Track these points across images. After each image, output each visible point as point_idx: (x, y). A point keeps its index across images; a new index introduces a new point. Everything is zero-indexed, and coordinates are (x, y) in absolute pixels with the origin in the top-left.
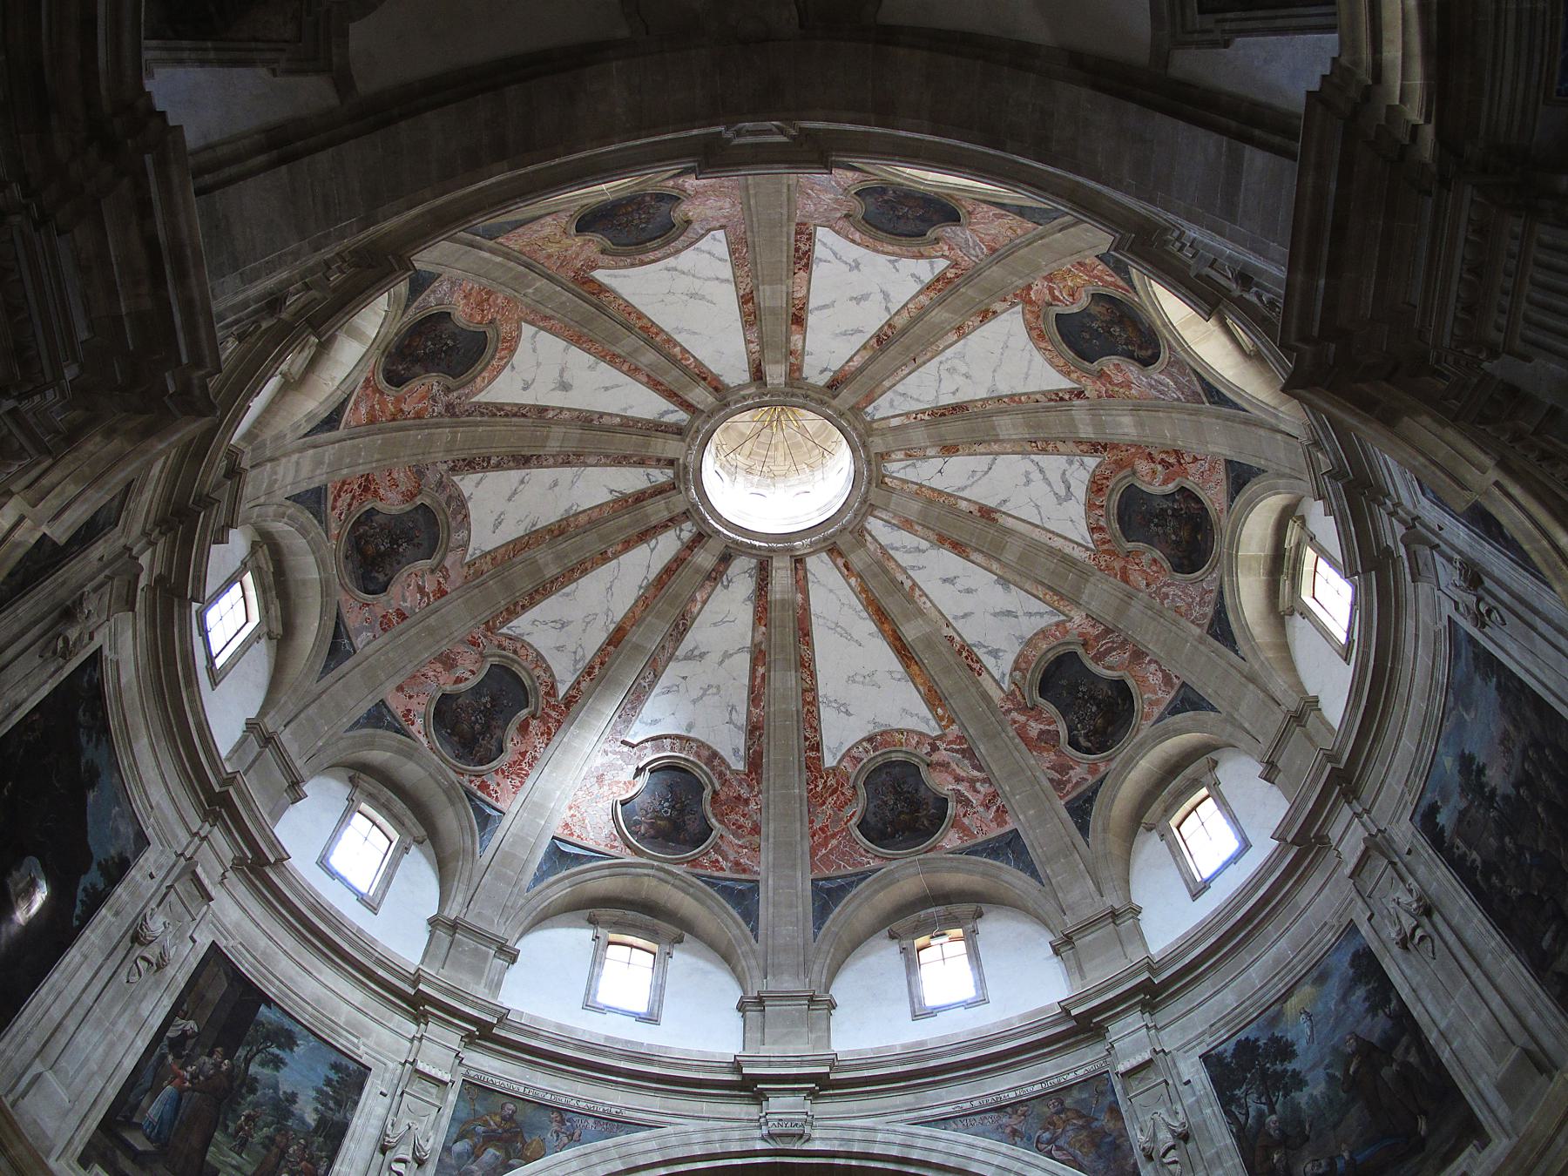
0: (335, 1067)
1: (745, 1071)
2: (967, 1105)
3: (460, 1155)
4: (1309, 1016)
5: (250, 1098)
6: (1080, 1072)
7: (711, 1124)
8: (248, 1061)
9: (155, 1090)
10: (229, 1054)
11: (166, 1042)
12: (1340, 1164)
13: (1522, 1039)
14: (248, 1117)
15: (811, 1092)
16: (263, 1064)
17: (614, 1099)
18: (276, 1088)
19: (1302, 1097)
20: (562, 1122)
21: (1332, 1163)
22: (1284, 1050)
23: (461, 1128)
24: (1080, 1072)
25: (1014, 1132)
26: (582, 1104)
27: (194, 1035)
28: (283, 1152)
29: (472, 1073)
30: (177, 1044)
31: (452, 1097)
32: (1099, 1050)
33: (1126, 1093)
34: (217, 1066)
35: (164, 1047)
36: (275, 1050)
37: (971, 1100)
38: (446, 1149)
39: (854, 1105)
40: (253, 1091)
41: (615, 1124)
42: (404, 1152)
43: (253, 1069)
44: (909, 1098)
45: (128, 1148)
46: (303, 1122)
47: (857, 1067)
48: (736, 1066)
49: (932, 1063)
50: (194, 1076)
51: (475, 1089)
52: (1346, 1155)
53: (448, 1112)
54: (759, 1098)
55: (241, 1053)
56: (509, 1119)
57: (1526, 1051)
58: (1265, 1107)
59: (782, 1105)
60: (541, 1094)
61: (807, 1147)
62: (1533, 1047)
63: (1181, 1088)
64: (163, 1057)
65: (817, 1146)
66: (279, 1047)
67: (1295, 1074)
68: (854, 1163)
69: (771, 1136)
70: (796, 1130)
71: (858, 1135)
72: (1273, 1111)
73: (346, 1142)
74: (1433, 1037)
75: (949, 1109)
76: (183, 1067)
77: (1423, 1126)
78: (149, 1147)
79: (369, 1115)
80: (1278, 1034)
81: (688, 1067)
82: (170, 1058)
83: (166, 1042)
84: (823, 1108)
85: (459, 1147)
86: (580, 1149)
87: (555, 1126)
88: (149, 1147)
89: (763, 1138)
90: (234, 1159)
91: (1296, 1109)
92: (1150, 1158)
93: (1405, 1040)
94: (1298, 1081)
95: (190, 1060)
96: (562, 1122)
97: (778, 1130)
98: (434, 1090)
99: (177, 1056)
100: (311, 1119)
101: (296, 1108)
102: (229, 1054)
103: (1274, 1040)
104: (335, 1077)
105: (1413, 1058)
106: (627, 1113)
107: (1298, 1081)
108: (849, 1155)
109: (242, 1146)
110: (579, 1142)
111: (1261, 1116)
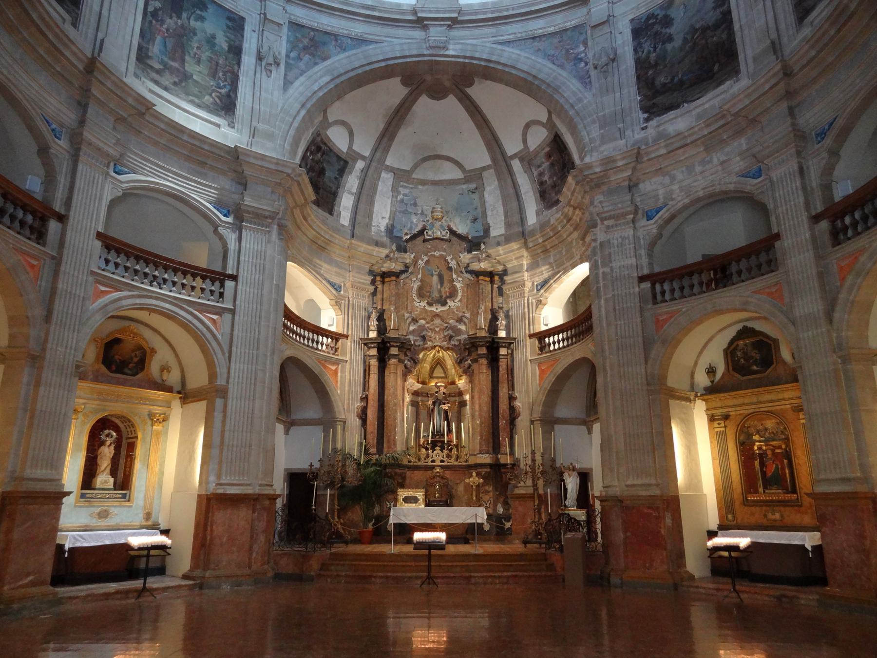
0: (229, 18)
1: (419, 15)
2: (519, 35)
3: (294, 59)
4: (685, 6)
5: (195, 38)
6: (573, 22)
7: (404, 41)
8: (189, 19)
9: (152, 40)
10: (179, 17)
11: (149, 14)
12: (676, 79)
13: (774, 36)
14: (198, 48)
15: (450, 26)
16: (196, 20)
17: (358, 29)
18: (206, 33)
19: (669, 47)
20: (336, 40)
21: (673, 79)
22: (667, 21)
23: (293, 45)
24: (573, 22)
25: (539, 50)
26: (345, 32)
27: (160, 9)
28: (217, 64)
29: (293, 17)
30: (155, 14)
31: (285, 29)
32: (583, 10)
33: (592, 33)
34: (176, 23)
35: (149, 18)
36: (199, 12)
37: (521, 33)
38: (287, 56)
39: (467, 33)
40: (195, 34)
41: (361, 41)
42: (271, 60)
43: (192, 22)
44: (493, 30)
45: (152, 67)
46: (221, 47)
47: (471, 14)
48: (415, 12)
49: (506, 13)
50: (167, 30)
51: (295, 26)
52: (680, 76)
53: (285, 38)
54: (425, 28)
55: (184, 15)
56: (312, 40)
57: (773, 43)
58: (652, 49)
59: (436, 33)
60: (325, 27)
61: (447, 53)
62: (777, 42)
63: (618, 35)
64: (151, 22)
65: (451, 53)
66: (201, 10)
67: (670, 35)
68: (467, 61)
69: (431, 47)
70: (442, 45)
71: (469, 48)
72: (655, 51)
73: (243, 56)
74: (736, 27)
75: (511, 37)
76: (161, 26)
77: (716, 68)
78: (161, 67)
79: (250, 43)
80: (668, 13)
81: (392, 12)
82: (154, 22)
83: (149, 14)
84: (455, 33)
85: (292, 55)
86: (347, 54)
87: (334, 43)
88: (161, 67)
89: (427, 48)
90: (198, 68)
91: (665, 51)
92: (596, 68)
93: (724, 26)
94: (670, 39)
95: (163, 22)
96: (336, 40)
97: (434, 44)
98: (277, 28)
99: (157, 21)
100: (225, 46)
101: (217, 41)
102: (179, 17)
103: (666, 17)
104: (230, 24)
105: (724, 36)
106: (365, 36)
107: (670, 39)
108: (465, 57)
109: (199, 62)
110: (345, 50)
111: (649, 52)
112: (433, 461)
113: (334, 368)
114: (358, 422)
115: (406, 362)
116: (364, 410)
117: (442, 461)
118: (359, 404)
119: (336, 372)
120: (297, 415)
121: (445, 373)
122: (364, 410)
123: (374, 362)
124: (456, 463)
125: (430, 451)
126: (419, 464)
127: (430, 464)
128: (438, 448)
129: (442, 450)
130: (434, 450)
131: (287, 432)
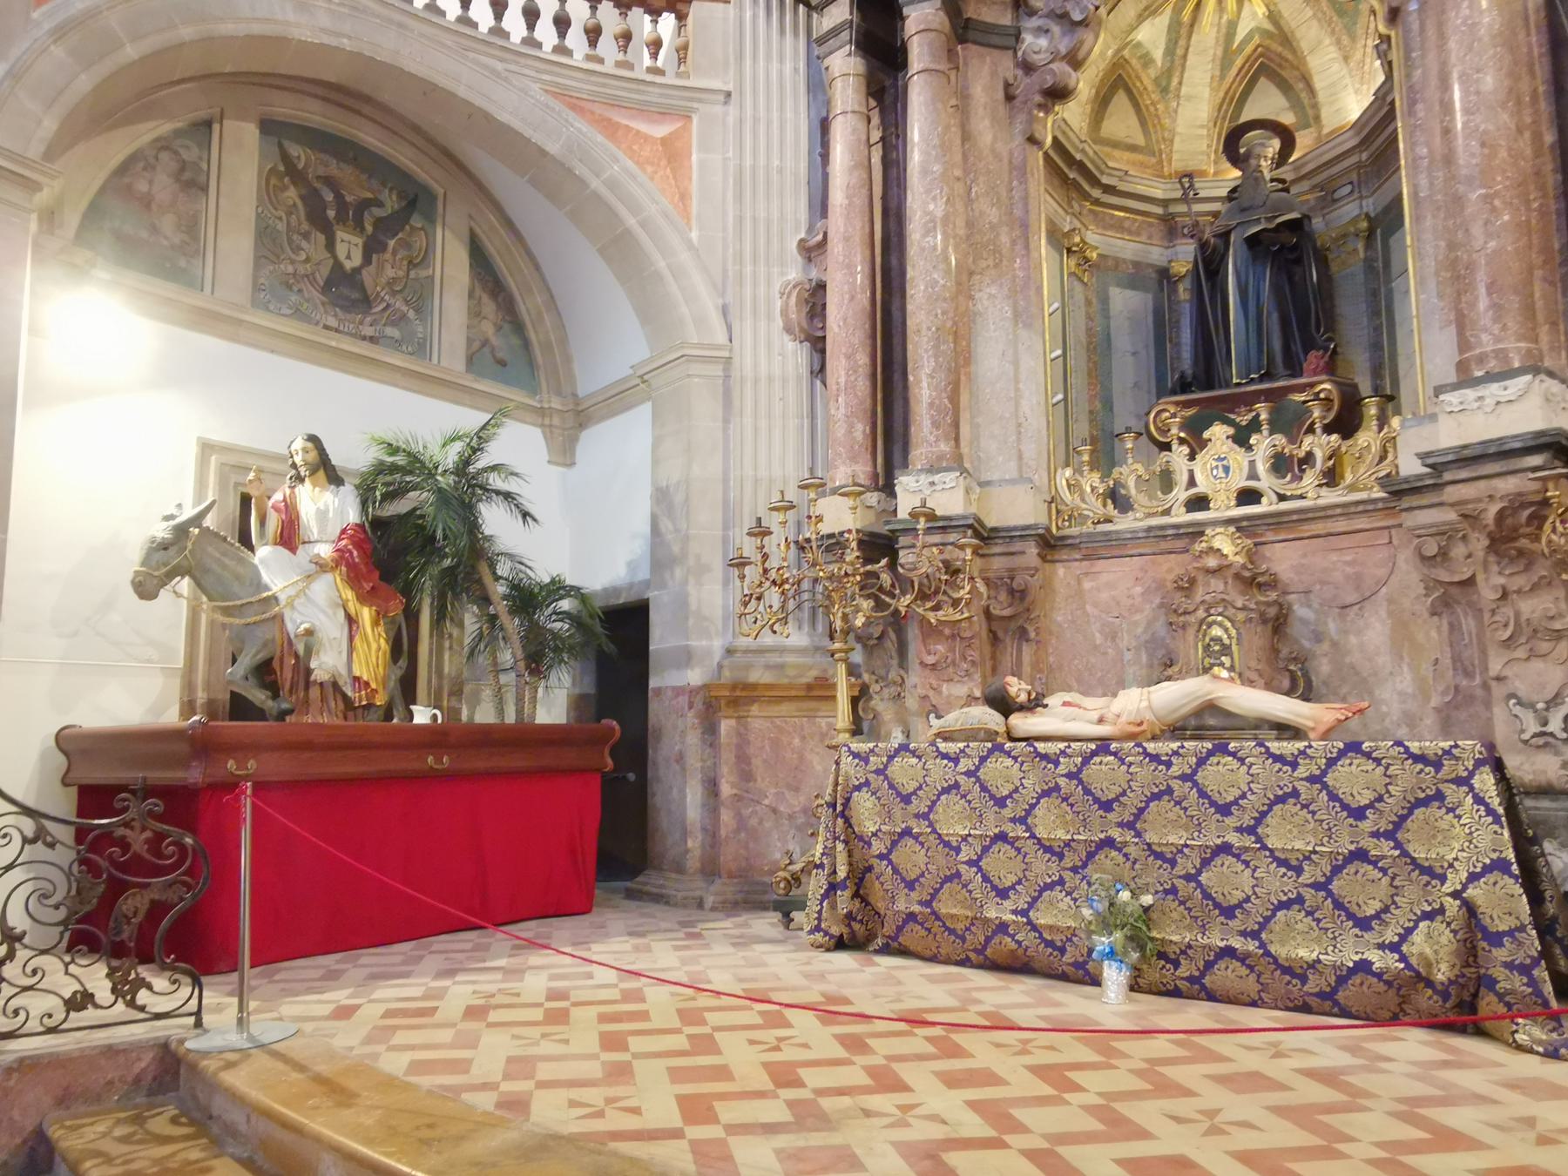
112: (1199, 503)
113: (660, 131)
114: (797, 355)
115: (1028, 38)
116: (815, 299)
117: (1248, 496)
118: (794, 271)
119: (673, 153)
120: (591, 379)
121: (1296, 105)
122: (815, 299)
123: (845, 65)
124: (1330, 497)
125: (1179, 453)
126: (1124, 523)
127: (1181, 516)
128: (1218, 433)
129: (1241, 439)
130: (1196, 444)
131: (564, 452)
